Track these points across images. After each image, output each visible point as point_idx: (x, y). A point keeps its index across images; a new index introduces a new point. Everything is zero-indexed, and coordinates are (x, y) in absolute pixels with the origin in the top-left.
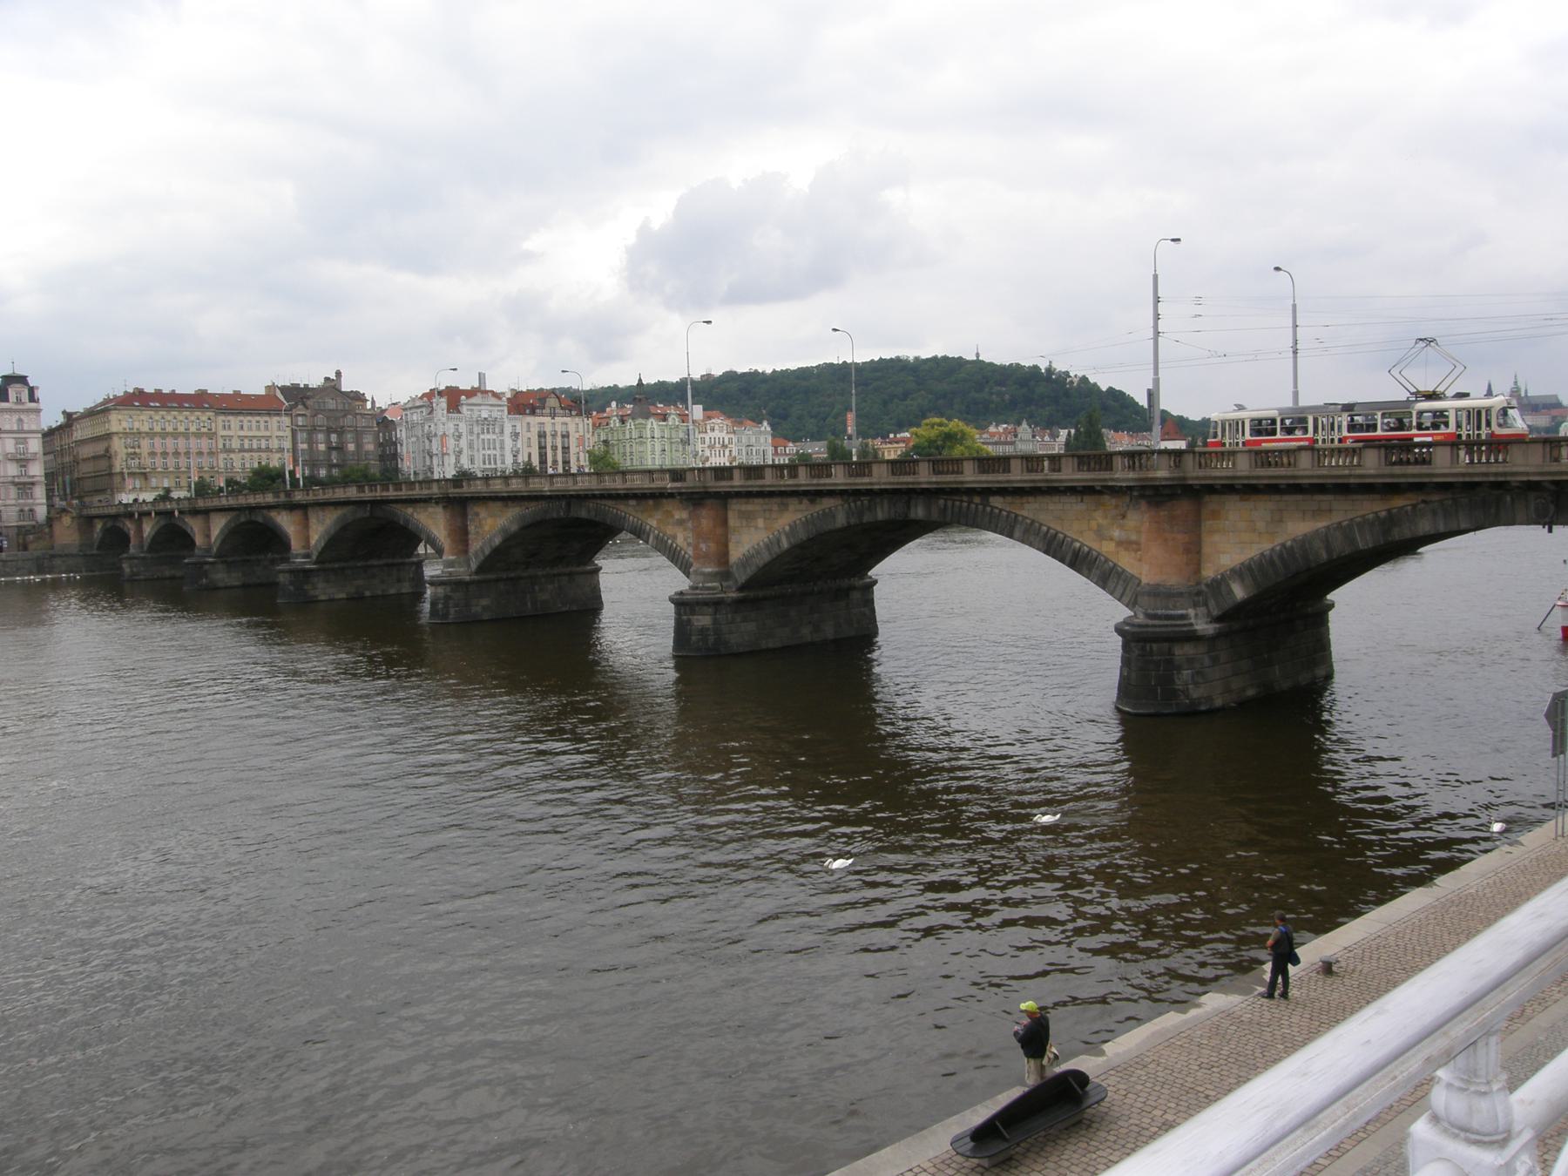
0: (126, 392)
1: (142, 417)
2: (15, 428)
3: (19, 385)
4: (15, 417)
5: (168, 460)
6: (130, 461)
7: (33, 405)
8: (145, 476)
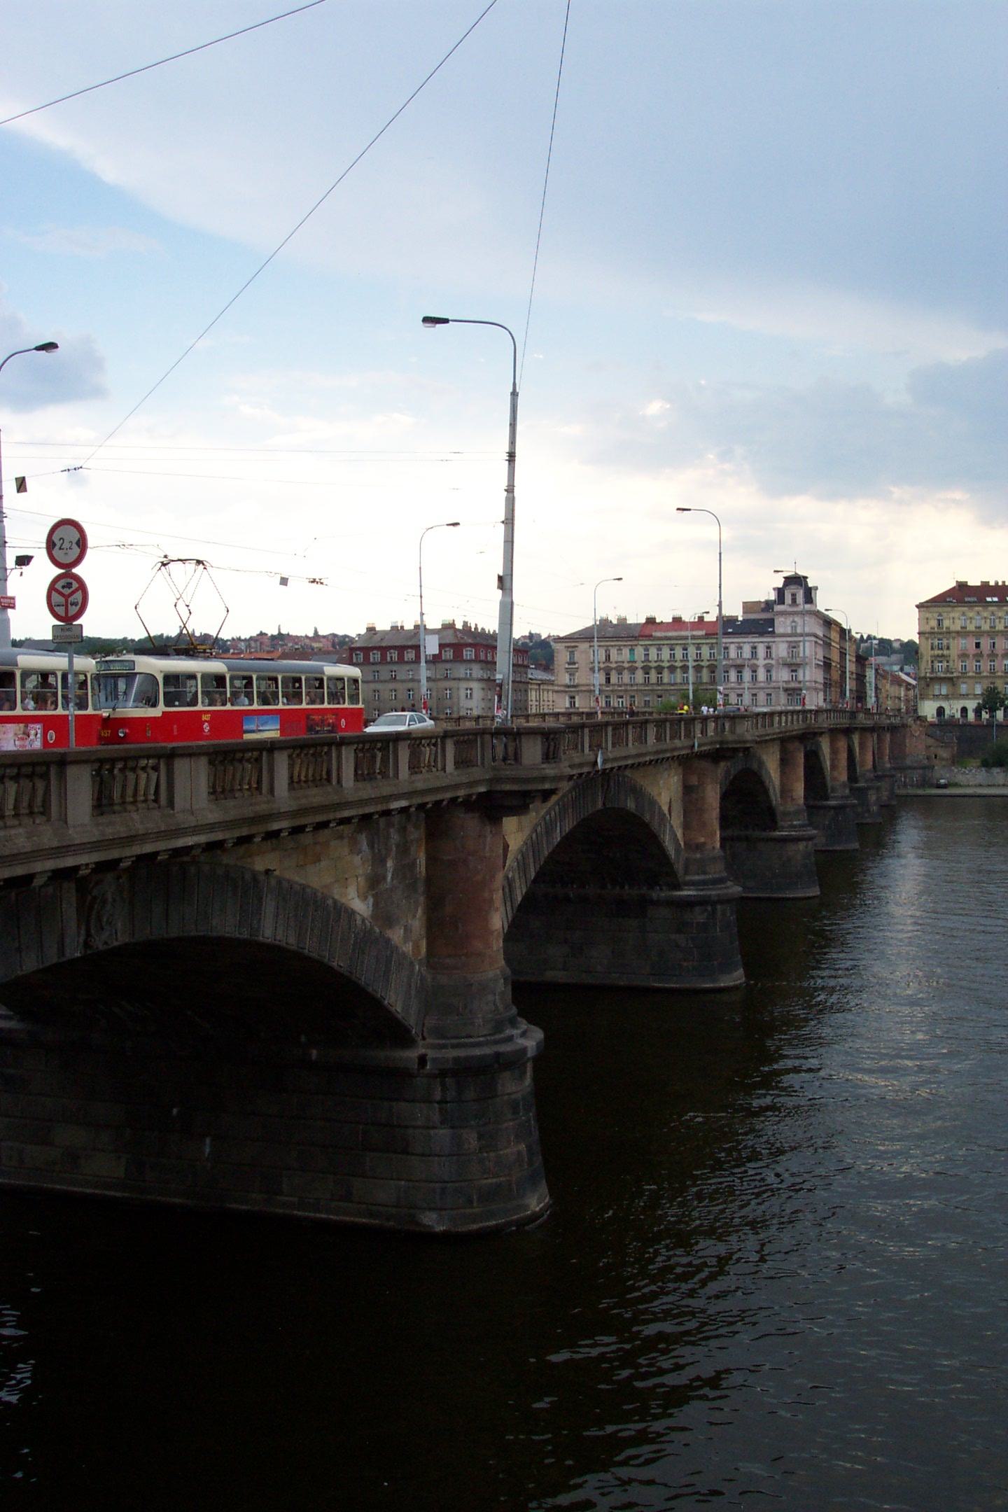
0: (997, 583)
1: (952, 615)
3: (792, 587)
6: (937, 664)
7: (808, 607)
8: (951, 681)
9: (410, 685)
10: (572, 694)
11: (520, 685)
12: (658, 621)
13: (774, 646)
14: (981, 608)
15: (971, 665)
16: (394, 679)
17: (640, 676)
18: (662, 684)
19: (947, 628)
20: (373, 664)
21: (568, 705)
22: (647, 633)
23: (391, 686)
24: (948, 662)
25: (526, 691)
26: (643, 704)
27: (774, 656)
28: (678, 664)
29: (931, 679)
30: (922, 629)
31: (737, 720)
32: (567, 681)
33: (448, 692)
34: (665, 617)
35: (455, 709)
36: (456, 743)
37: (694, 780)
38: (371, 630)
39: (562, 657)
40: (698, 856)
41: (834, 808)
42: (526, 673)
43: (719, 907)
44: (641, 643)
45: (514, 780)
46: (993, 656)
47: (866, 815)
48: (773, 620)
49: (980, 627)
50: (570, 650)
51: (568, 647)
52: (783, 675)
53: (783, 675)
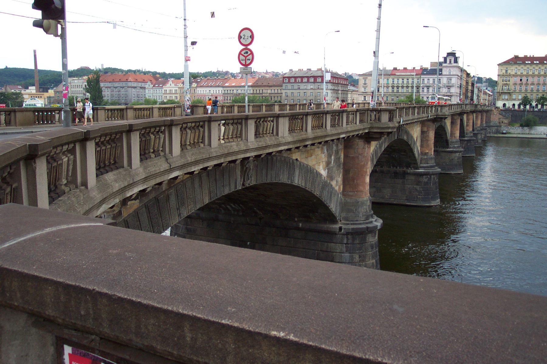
0: (530, 56)
1: (511, 68)
2: (448, 74)
3: (450, 57)
4: (448, 69)
5: (540, 87)
6: (504, 87)
7: (455, 64)
8: (509, 93)
9: (305, 91)
10: (365, 96)
11: (345, 92)
12: (398, 69)
13: (441, 79)
14: (523, 66)
15: (518, 88)
16: (299, 89)
17: (390, 89)
18: (399, 93)
19: (510, 73)
20: (292, 83)
21: (363, 100)
22: (394, 73)
23: (298, 91)
24: (509, 86)
25: (347, 94)
26: (391, 100)
27: (441, 83)
28: (405, 85)
29: (501, 93)
30: (499, 74)
31: (443, 107)
32: (363, 91)
33: (319, 94)
34: (400, 67)
35: (321, 100)
36: (360, 113)
37: (425, 129)
38: (291, 70)
39: (361, 82)
40: (426, 157)
41: (467, 140)
42: (347, 87)
43: (432, 176)
44: (391, 77)
45: (378, 128)
46: (527, 84)
47: (477, 143)
48: (442, 69)
49: (522, 73)
50: (365, 79)
51: (363, 78)
52: (444, 90)
53: (444, 90)
